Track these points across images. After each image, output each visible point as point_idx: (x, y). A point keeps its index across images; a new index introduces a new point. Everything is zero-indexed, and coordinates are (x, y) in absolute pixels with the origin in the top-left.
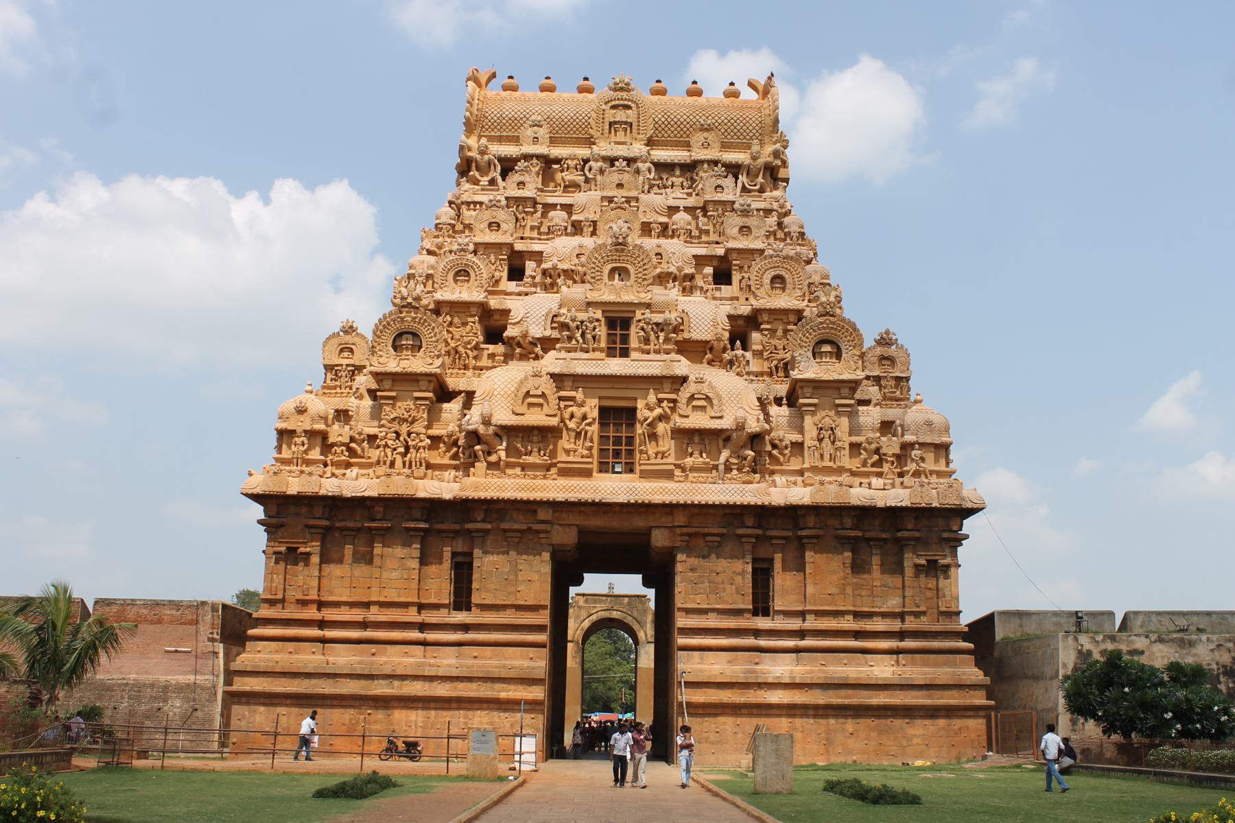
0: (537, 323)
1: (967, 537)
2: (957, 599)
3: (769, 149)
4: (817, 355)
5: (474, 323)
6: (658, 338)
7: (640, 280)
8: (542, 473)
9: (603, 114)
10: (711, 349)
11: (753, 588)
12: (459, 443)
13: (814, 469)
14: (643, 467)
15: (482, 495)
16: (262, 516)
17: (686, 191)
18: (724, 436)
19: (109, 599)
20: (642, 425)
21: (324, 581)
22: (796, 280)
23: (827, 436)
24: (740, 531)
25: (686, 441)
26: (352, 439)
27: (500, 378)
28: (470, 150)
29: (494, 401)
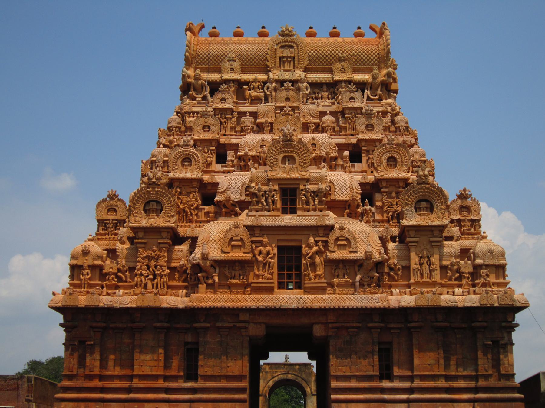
0: (236, 191)
1: (517, 325)
2: (512, 365)
4: (418, 210)
5: (195, 192)
6: (314, 201)
7: (302, 164)
8: (242, 290)
9: (275, 52)
10: (349, 206)
11: (379, 362)
12: (188, 271)
13: (417, 283)
15: (204, 305)
16: (62, 321)
18: (358, 264)
22: (403, 159)
23: (425, 262)
24: (370, 325)
25: (334, 267)
26: (119, 270)
27: (213, 229)
28: (189, 77)
29: (209, 244)
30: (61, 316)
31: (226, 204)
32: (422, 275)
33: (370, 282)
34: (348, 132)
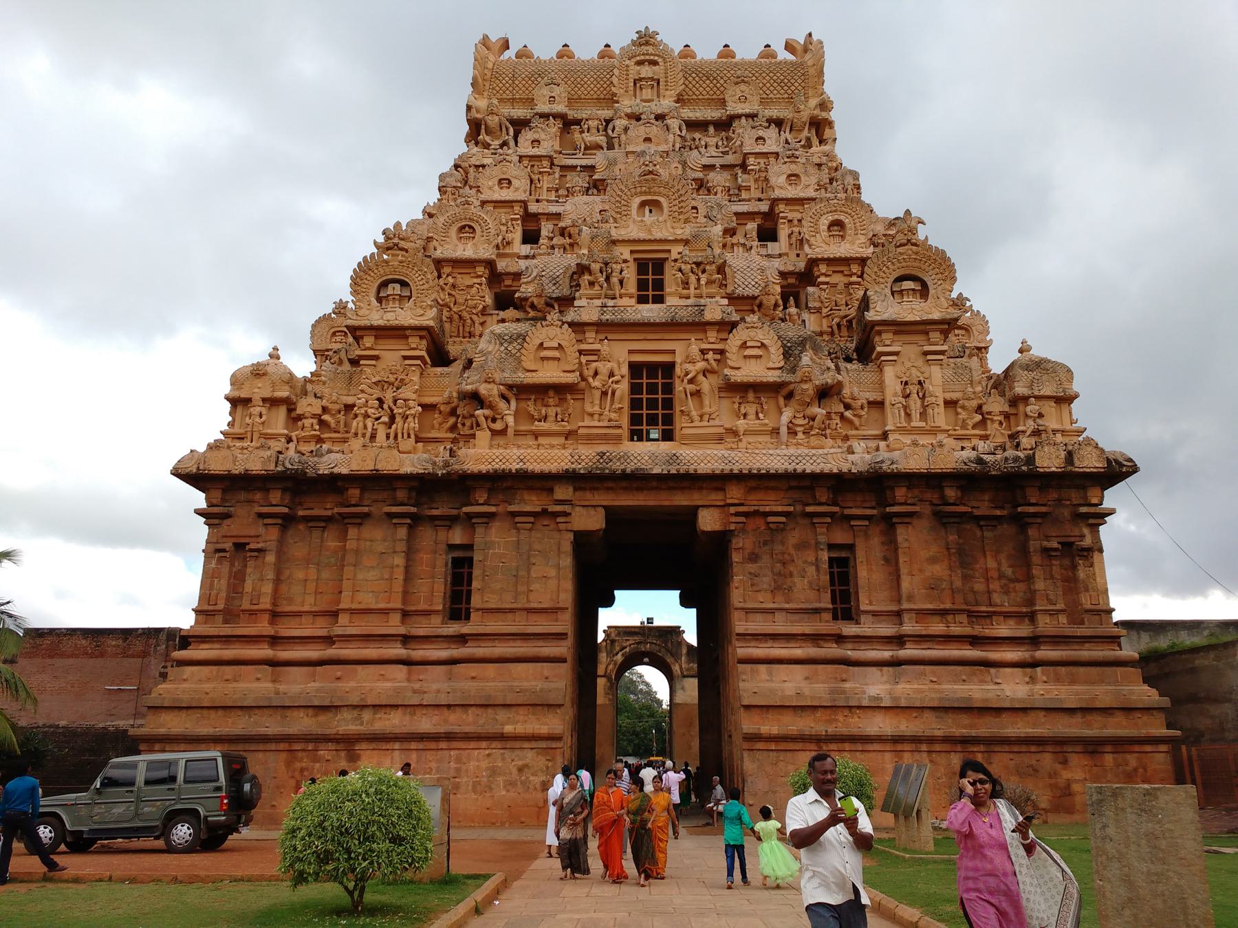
3: (813, 102)
5: (480, 284)
6: (699, 280)
9: (627, 71)
10: (760, 306)
14: (685, 431)
15: (484, 468)
16: (203, 504)
17: (721, 150)
18: (785, 391)
19: (44, 629)
20: (683, 381)
21: (284, 588)
22: (858, 224)
24: (809, 509)
25: (737, 400)
26: (325, 409)
28: (478, 111)
30: (201, 496)
31: (536, 303)
32: (908, 415)
33: (807, 426)
34: (753, 196)
